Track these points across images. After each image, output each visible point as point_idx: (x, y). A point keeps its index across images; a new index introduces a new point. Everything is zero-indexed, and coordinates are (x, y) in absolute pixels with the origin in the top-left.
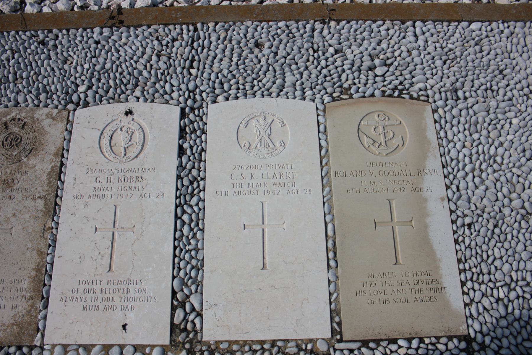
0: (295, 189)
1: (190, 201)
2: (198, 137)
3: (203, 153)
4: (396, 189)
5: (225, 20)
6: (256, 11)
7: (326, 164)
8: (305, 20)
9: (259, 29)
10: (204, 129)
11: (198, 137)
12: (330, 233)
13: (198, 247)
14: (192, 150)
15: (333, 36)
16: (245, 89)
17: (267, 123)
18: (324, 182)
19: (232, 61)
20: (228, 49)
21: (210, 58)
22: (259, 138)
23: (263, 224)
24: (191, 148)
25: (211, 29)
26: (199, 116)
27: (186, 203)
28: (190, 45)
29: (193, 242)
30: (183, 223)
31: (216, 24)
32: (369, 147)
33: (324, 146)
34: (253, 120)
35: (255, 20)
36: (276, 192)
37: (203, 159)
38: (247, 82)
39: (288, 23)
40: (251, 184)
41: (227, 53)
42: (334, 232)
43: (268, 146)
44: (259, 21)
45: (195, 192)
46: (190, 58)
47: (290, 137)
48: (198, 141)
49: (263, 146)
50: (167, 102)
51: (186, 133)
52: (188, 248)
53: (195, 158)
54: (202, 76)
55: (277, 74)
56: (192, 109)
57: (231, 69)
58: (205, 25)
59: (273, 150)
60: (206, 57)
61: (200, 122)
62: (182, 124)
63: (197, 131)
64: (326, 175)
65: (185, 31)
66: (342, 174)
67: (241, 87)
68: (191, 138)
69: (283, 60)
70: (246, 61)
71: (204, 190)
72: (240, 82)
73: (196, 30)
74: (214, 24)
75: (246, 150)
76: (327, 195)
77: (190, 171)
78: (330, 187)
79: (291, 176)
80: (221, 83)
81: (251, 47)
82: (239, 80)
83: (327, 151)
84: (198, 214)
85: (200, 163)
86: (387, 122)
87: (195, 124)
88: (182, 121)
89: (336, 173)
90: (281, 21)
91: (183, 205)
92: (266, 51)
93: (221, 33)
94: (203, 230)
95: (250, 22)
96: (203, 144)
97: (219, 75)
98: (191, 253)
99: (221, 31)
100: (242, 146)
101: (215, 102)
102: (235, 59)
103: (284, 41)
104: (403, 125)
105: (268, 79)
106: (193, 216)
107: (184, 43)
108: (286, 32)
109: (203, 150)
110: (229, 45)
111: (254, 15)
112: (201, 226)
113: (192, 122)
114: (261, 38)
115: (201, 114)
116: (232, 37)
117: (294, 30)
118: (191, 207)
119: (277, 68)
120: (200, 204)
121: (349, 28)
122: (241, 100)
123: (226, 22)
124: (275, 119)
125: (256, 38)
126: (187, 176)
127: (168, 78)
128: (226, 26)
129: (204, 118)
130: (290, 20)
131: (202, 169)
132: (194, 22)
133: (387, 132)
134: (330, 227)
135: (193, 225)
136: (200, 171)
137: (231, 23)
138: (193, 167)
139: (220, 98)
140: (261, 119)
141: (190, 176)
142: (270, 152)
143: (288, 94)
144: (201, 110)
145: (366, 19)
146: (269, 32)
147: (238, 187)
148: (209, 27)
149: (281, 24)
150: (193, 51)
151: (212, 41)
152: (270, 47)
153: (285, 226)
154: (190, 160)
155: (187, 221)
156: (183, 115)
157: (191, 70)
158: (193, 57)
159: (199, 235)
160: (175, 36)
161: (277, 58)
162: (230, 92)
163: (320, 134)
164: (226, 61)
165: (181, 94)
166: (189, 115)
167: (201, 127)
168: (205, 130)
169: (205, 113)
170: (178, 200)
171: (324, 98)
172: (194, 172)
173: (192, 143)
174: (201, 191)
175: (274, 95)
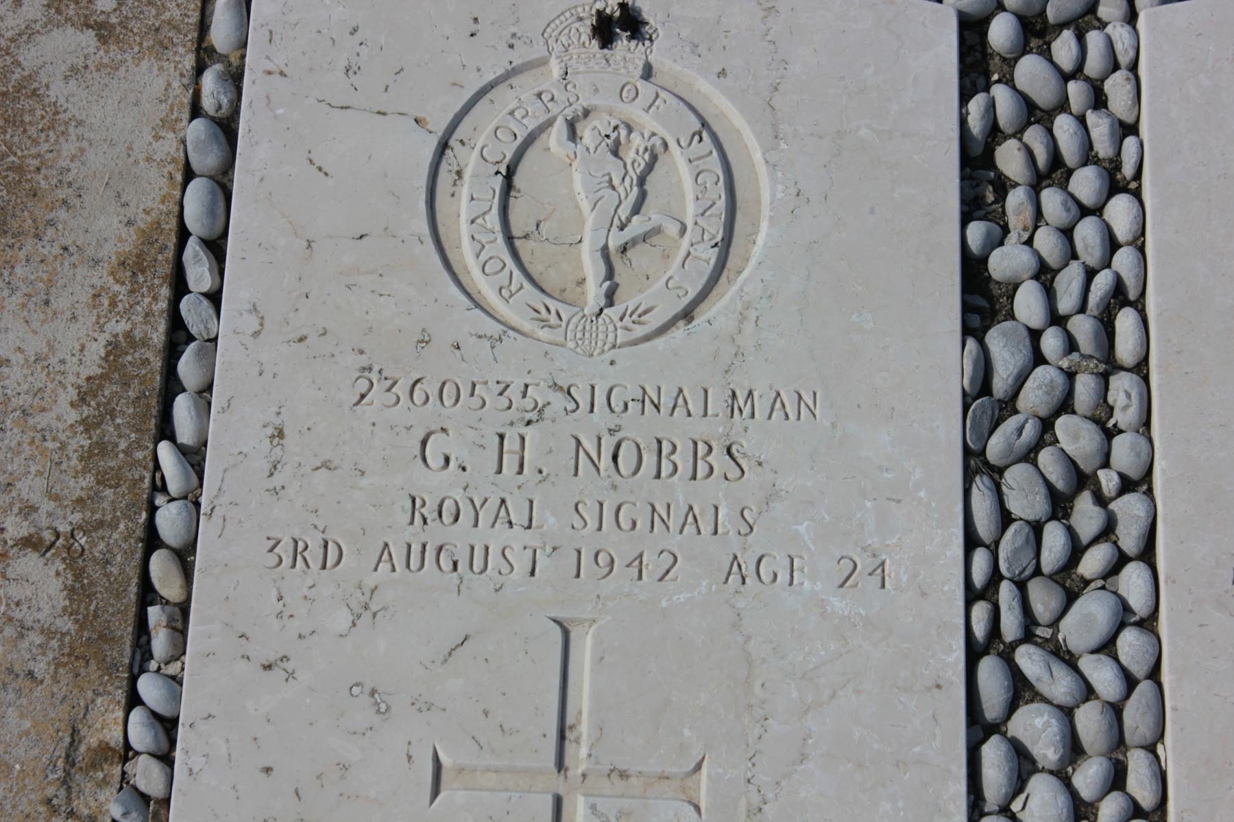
1: (1055, 624)
2: (1085, 211)
3: (1126, 321)
10: (1113, 166)
11: (1085, 211)
14: (1050, 293)
24: (1045, 274)
26: (1078, 72)
27: (1028, 636)
37: (1126, 348)
45: (1093, 562)
48: (1087, 232)
51: (1003, 186)
53: (1071, 345)
61: (1091, 117)
62: (976, 124)
63: (1070, 172)
68: (1039, 214)
71: (1147, 554)
77: (1047, 424)
84: (1116, 710)
85: (1105, 377)
87: (1064, 126)
88: (976, 105)
91: (1013, 646)
96: (1124, 260)
106: (1090, 721)
109: (1119, 296)
115: (1094, 64)
118: (1070, 660)
120: (1130, 643)
126: (1030, 456)
129: (1117, 88)
131: (1124, 416)
135: (1088, 777)
136: (1110, 434)
138: (1066, 405)
141: (1046, 457)
144: (1094, 39)
154: (1039, 359)
155: (1047, 751)
166: (1010, 62)
167: (1103, 148)
168: (1128, 170)
169: (1124, 59)
170: (980, 612)
173: (1047, 242)
174: (1122, 560)
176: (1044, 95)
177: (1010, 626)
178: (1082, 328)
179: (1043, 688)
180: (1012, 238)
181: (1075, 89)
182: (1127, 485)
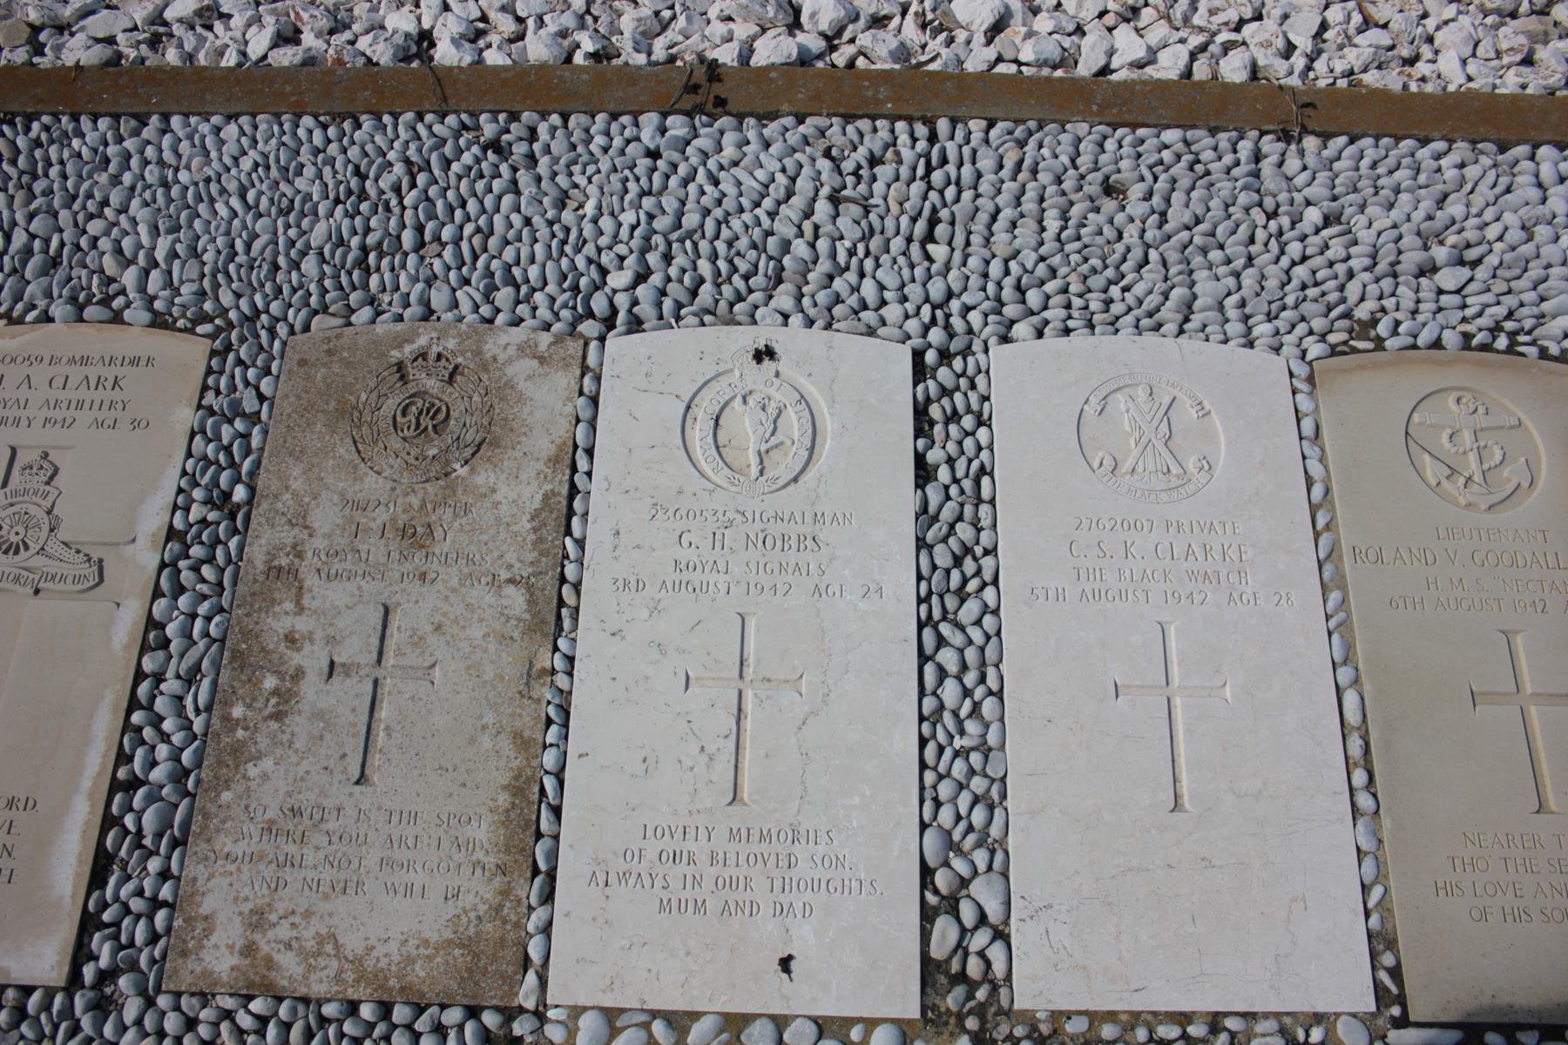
0: (1249, 590)
1: (956, 613)
2: (967, 434)
3: (985, 481)
4: (1522, 604)
5: (1013, 116)
6: (1099, 97)
7: (1328, 527)
8: (1235, 129)
9: (1110, 145)
10: (980, 414)
11: (967, 434)
12: (1353, 716)
13: (986, 743)
14: (953, 469)
15: (1314, 179)
16: (1086, 308)
17: (1157, 405)
18: (1326, 575)
19: (1043, 229)
20: (1031, 194)
21: (983, 217)
22: (1141, 447)
23: (1167, 684)
24: (951, 461)
25: (977, 137)
26: (964, 374)
27: (944, 618)
28: (922, 179)
29: (972, 727)
30: (942, 673)
31: (991, 124)
32: (1438, 484)
33: (1316, 478)
34: (1119, 395)
35: (1097, 120)
36: (1197, 598)
37: (986, 493)
38: (1090, 291)
39: (1189, 134)
40: (1128, 572)
41: (1029, 205)
42: (1364, 716)
43: (1165, 470)
44: (1108, 124)
45: (972, 586)
46: (926, 212)
47: (1223, 447)
48: (969, 443)
49: (1151, 467)
50: (871, 332)
51: (932, 423)
52: (958, 742)
53: (962, 492)
54: (964, 265)
55: (1173, 271)
56: (945, 356)
57: (1043, 250)
58: (960, 126)
59: (1181, 482)
60: (971, 214)
61: (970, 393)
62: (920, 396)
63: (961, 417)
64: (1329, 557)
65: (903, 138)
66: (1372, 556)
67: (1077, 302)
69: (1185, 235)
70: (1083, 231)
71: (995, 582)
72: (1072, 289)
73: (933, 138)
74: (984, 123)
75: (1107, 478)
76: (1337, 611)
77: (952, 526)
78: (1343, 588)
79: (1235, 557)
80: (1020, 289)
81: (1093, 195)
82: (1068, 284)
83: (1327, 491)
84: (982, 649)
85: (977, 506)
86: (1481, 420)
87: (958, 397)
88: (920, 388)
89: (1357, 551)
90: (1168, 127)
91: (938, 623)
92: (1136, 208)
93: (1007, 151)
94: (999, 695)
95: (1085, 126)
96: (984, 455)
97: (1013, 265)
98: (967, 759)
99: (1006, 146)
100: (1096, 465)
101: (1005, 339)
102: (1052, 224)
103: (1185, 183)
104: (1527, 429)
105: (1150, 284)
106: (971, 655)
107: (904, 171)
108: (1185, 158)
109: (982, 470)
110: (1030, 186)
111: (1095, 108)
112: (992, 682)
113: (945, 392)
114: (1119, 171)
115: (971, 371)
116: (1037, 164)
117: (1207, 155)
118: (962, 629)
119: (1172, 257)
120: (988, 621)
121: (1358, 156)
122: (1079, 339)
123: (1017, 122)
124: (1180, 395)
125: (1106, 170)
126: (945, 540)
127: (869, 264)
128: (1019, 132)
129: (980, 381)
130: (1193, 127)
132: (929, 115)
133: (1486, 446)
134: (1350, 698)
135: (970, 678)
136: (979, 530)
137: (1032, 124)
138: (960, 518)
139: (1021, 330)
140: (1141, 393)
141: (952, 540)
142: (1173, 484)
143: (1208, 329)
144: (970, 359)
145: (1401, 133)
146: (1139, 155)
147: (1091, 577)
148: (970, 133)
149: (1171, 136)
150: (933, 195)
151: (983, 172)
152: (1148, 196)
153: (1228, 692)
154: (948, 498)
155: (952, 667)
156: (920, 371)
157: (930, 247)
158: (934, 210)
159: (988, 707)
160: (877, 151)
161: (1167, 227)
162: (1047, 314)
163: (1304, 442)
164: (1026, 230)
165: (911, 312)
166: (935, 370)
167: (975, 406)
168: (986, 416)
169: (983, 368)
170: (923, 608)
171: (1305, 344)
172: (964, 531)
173: (951, 447)
174: (984, 585)
175: (1171, 328)
176: (949, 384)
177: (937, 614)
178: (967, 484)
179: (951, 640)
180: (937, 445)
181: (963, 381)
182: (986, 552)
